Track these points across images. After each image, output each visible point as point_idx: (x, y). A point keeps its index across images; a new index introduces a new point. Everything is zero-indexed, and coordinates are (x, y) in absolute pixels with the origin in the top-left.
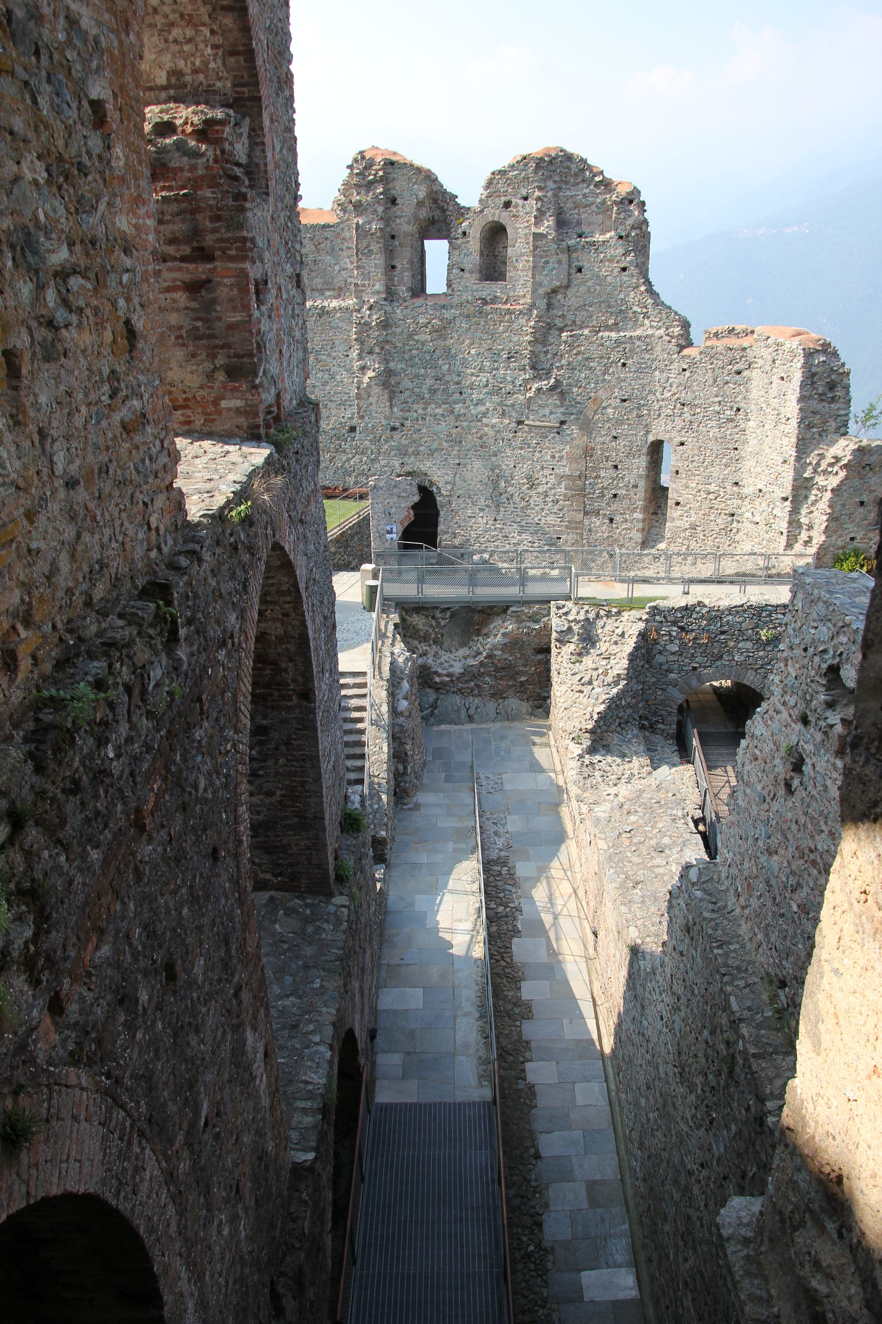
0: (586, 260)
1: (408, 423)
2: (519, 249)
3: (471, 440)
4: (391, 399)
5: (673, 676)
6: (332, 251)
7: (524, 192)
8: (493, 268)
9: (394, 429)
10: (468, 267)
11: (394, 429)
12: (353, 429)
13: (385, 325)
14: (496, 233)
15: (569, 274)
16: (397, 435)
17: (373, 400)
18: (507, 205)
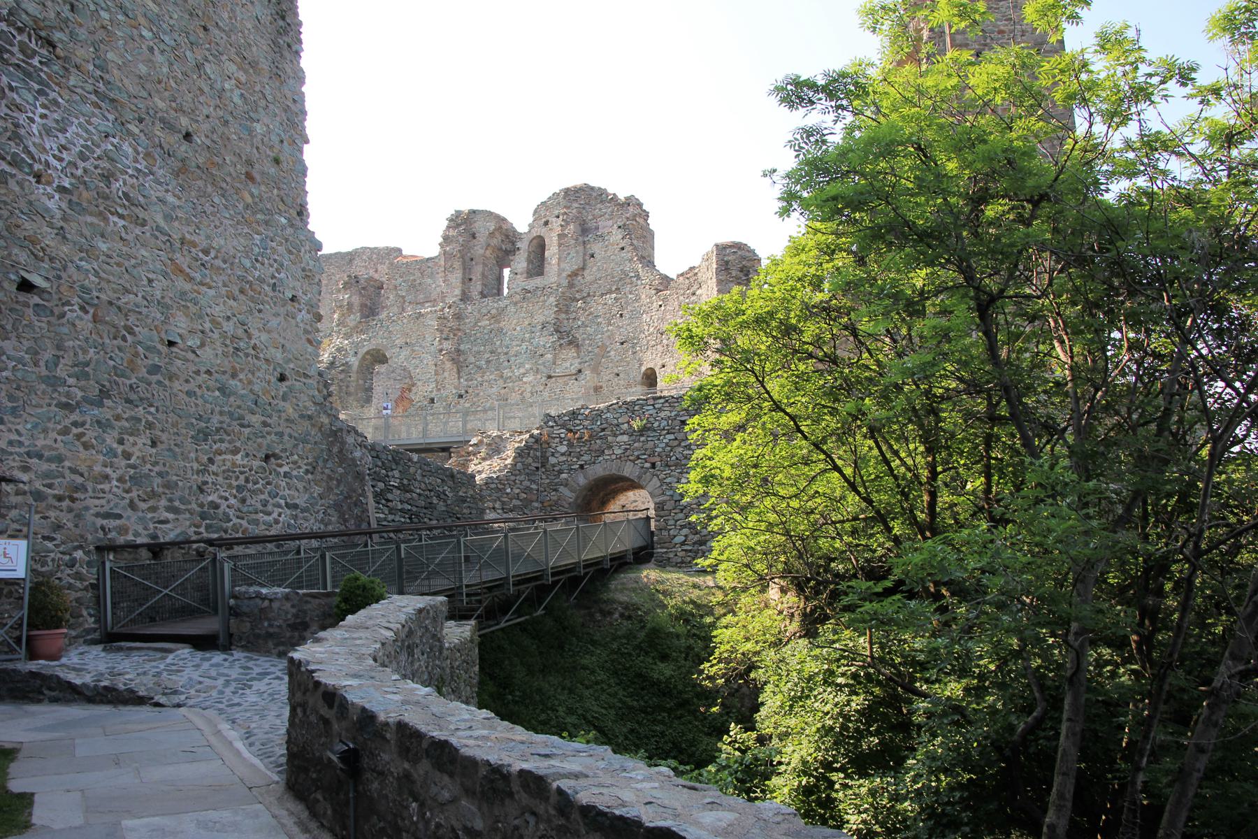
0: (596, 248)
1: (470, 390)
2: (552, 252)
3: (514, 398)
4: (459, 372)
5: (564, 476)
6: (431, 276)
7: (556, 212)
8: (537, 264)
9: (461, 396)
10: (519, 271)
11: (461, 396)
12: (432, 400)
13: (458, 317)
14: (539, 246)
15: (584, 261)
16: (462, 401)
17: (446, 374)
18: (546, 223)
